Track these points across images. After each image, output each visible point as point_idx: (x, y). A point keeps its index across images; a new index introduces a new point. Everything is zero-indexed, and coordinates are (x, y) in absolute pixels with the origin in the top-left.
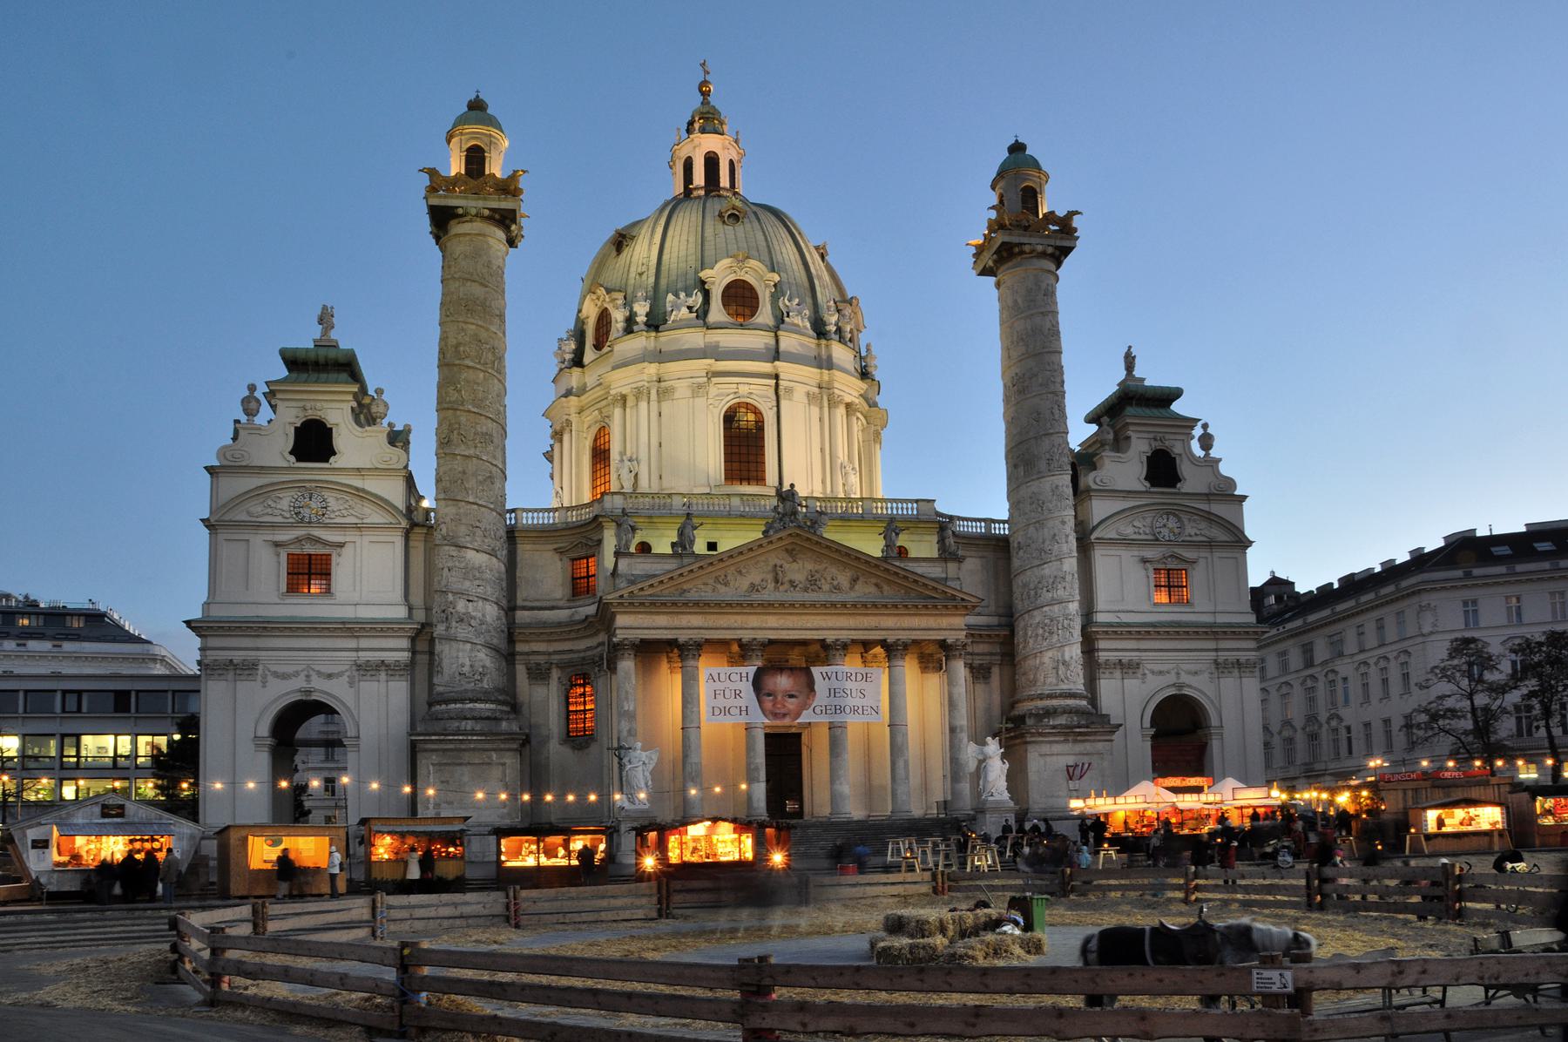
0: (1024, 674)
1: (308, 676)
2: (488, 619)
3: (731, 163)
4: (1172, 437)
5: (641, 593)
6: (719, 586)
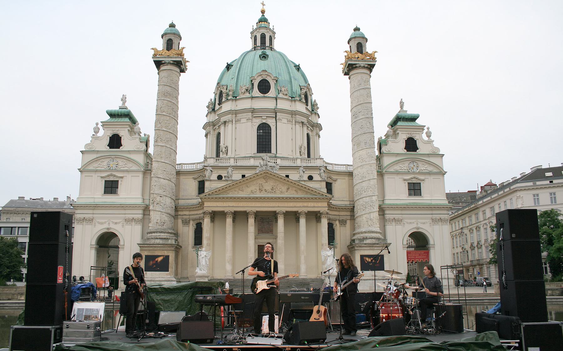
0: (357, 223)
1: (109, 223)
2: (168, 204)
3: (270, 37)
5: (213, 194)
6: (240, 191)
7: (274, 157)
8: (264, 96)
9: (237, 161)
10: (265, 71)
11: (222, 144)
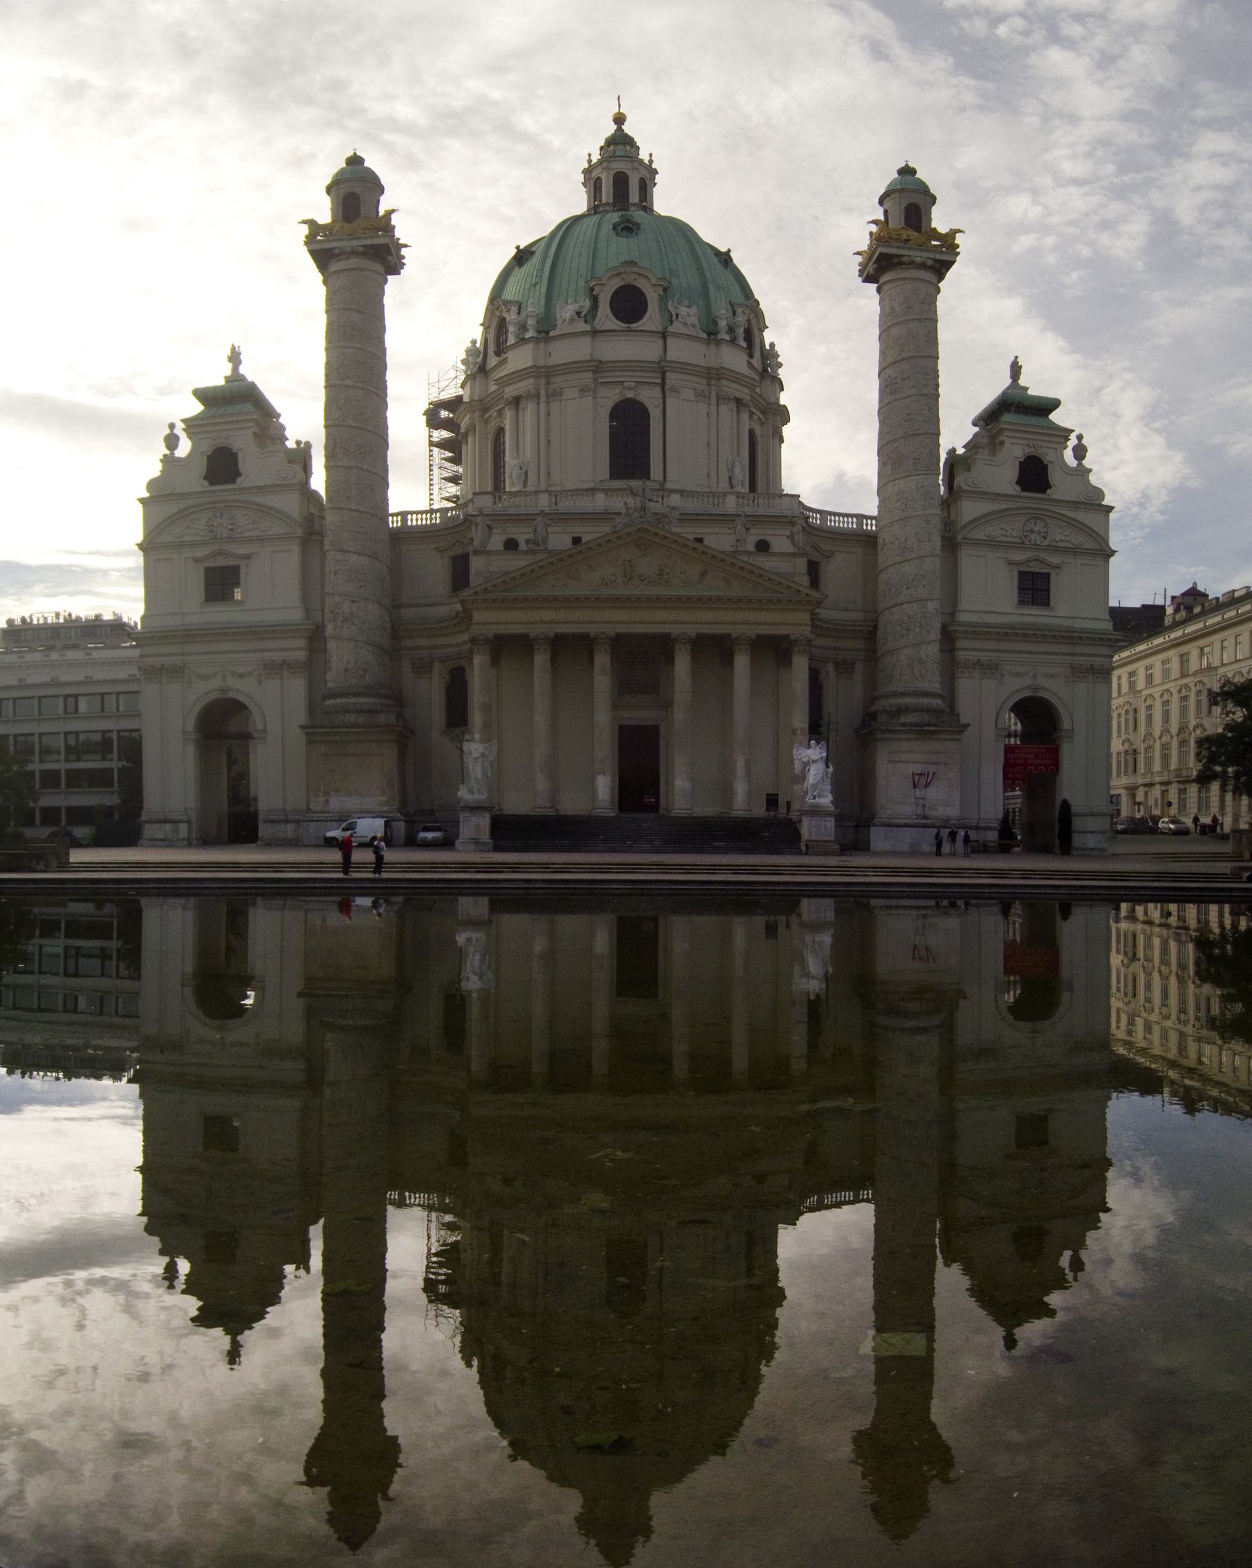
4: (1045, 444)
7: (659, 490)
8: (629, 327)
9: (558, 499)
10: (632, 263)
11: (510, 460)
